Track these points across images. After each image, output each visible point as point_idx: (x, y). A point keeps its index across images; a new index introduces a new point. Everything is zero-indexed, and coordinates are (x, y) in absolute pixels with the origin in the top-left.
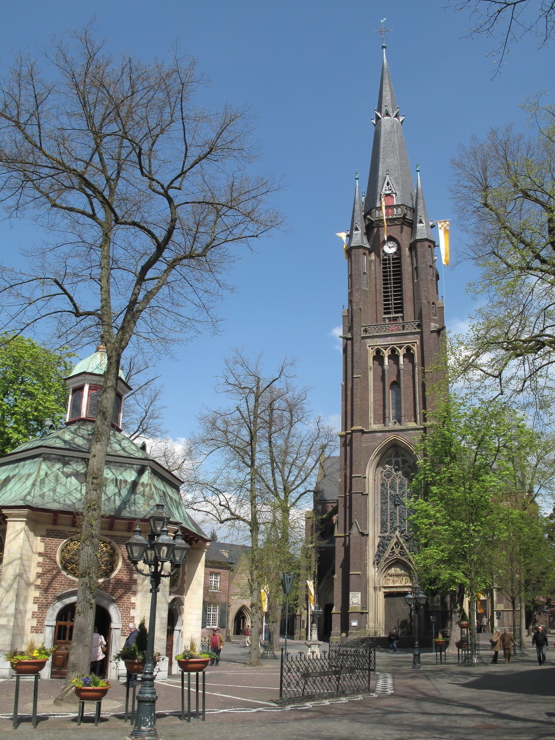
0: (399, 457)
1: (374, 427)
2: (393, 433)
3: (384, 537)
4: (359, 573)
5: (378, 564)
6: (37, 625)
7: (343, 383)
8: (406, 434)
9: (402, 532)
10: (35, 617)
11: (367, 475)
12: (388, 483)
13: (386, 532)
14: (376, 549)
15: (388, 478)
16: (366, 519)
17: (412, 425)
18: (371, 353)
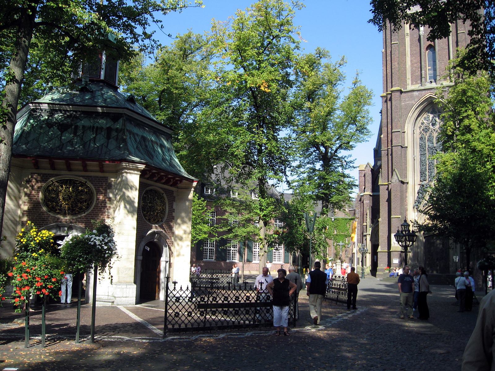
1: (410, 87)
2: (429, 91)
3: (423, 185)
4: (400, 216)
7: (383, 50)
11: (406, 130)
12: (427, 137)
13: (425, 181)
14: (417, 195)
15: (426, 132)
16: (406, 169)
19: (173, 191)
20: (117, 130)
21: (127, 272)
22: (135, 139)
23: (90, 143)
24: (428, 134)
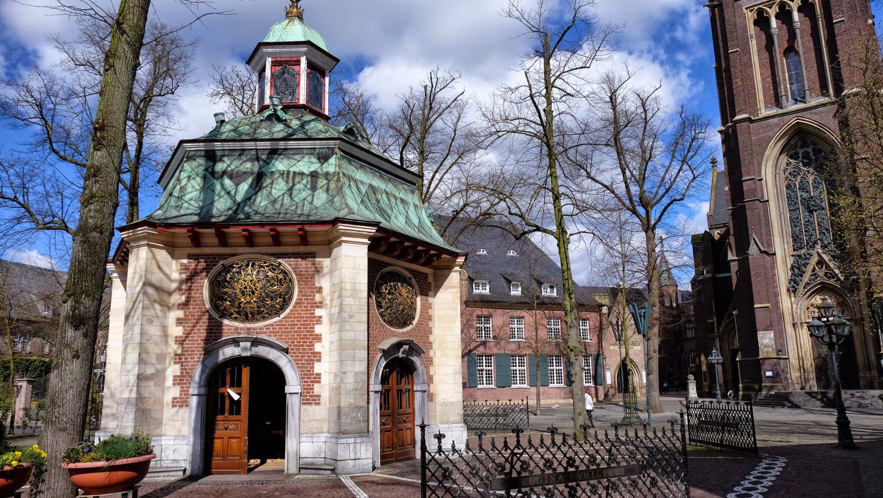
0: (808, 146)
1: (764, 113)
2: (795, 115)
3: (799, 256)
5: (794, 292)
6: (181, 394)
8: (815, 113)
9: (824, 247)
10: (178, 384)
11: (763, 176)
12: (797, 183)
13: (802, 248)
14: (790, 273)
15: (795, 176)
16: (769, 233)
17: (823, 100)
18: (751, 17)
19: (427, 274)
20: (327, 174)
21: (354, 414)
22: (358, 189)
23: (283, 200)
24: (799, 178)
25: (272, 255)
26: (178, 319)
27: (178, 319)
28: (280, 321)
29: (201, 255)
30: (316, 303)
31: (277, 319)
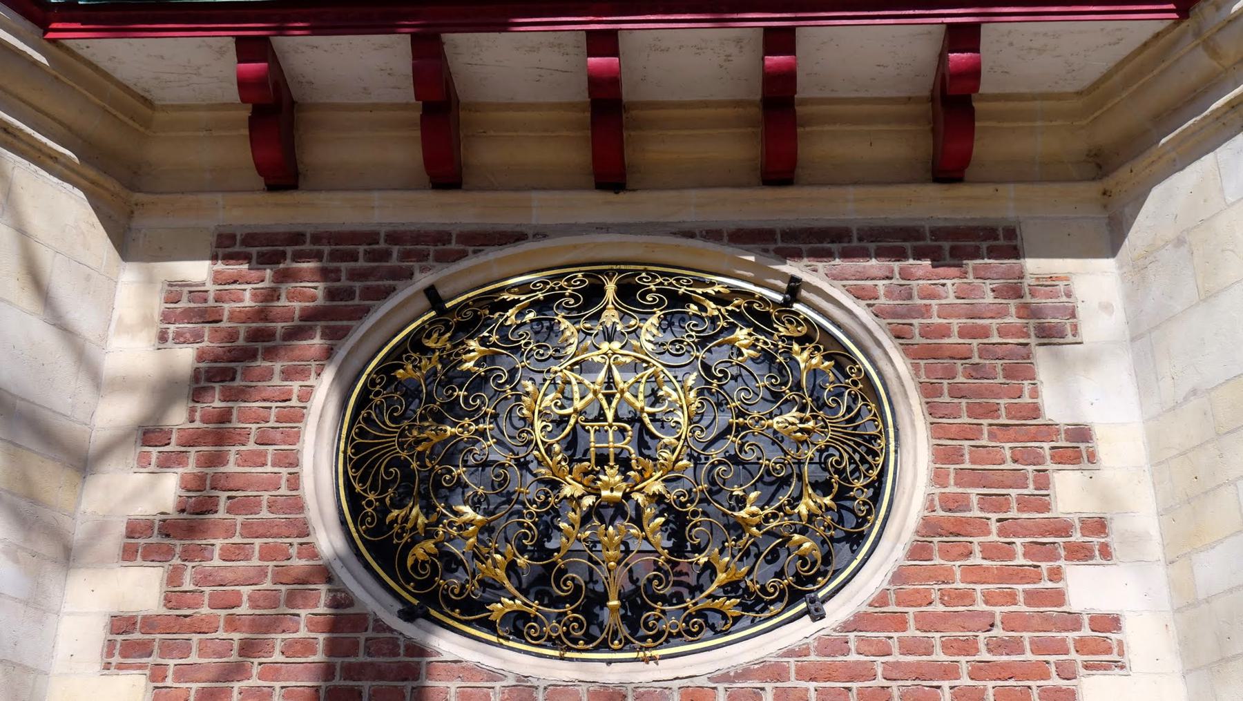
25: (744, 237)
26: (121, 624)
27: (121, 624)
28: (830, 646)
29: (296, 238)
30: (1063, 528)
31: (802, 631)
